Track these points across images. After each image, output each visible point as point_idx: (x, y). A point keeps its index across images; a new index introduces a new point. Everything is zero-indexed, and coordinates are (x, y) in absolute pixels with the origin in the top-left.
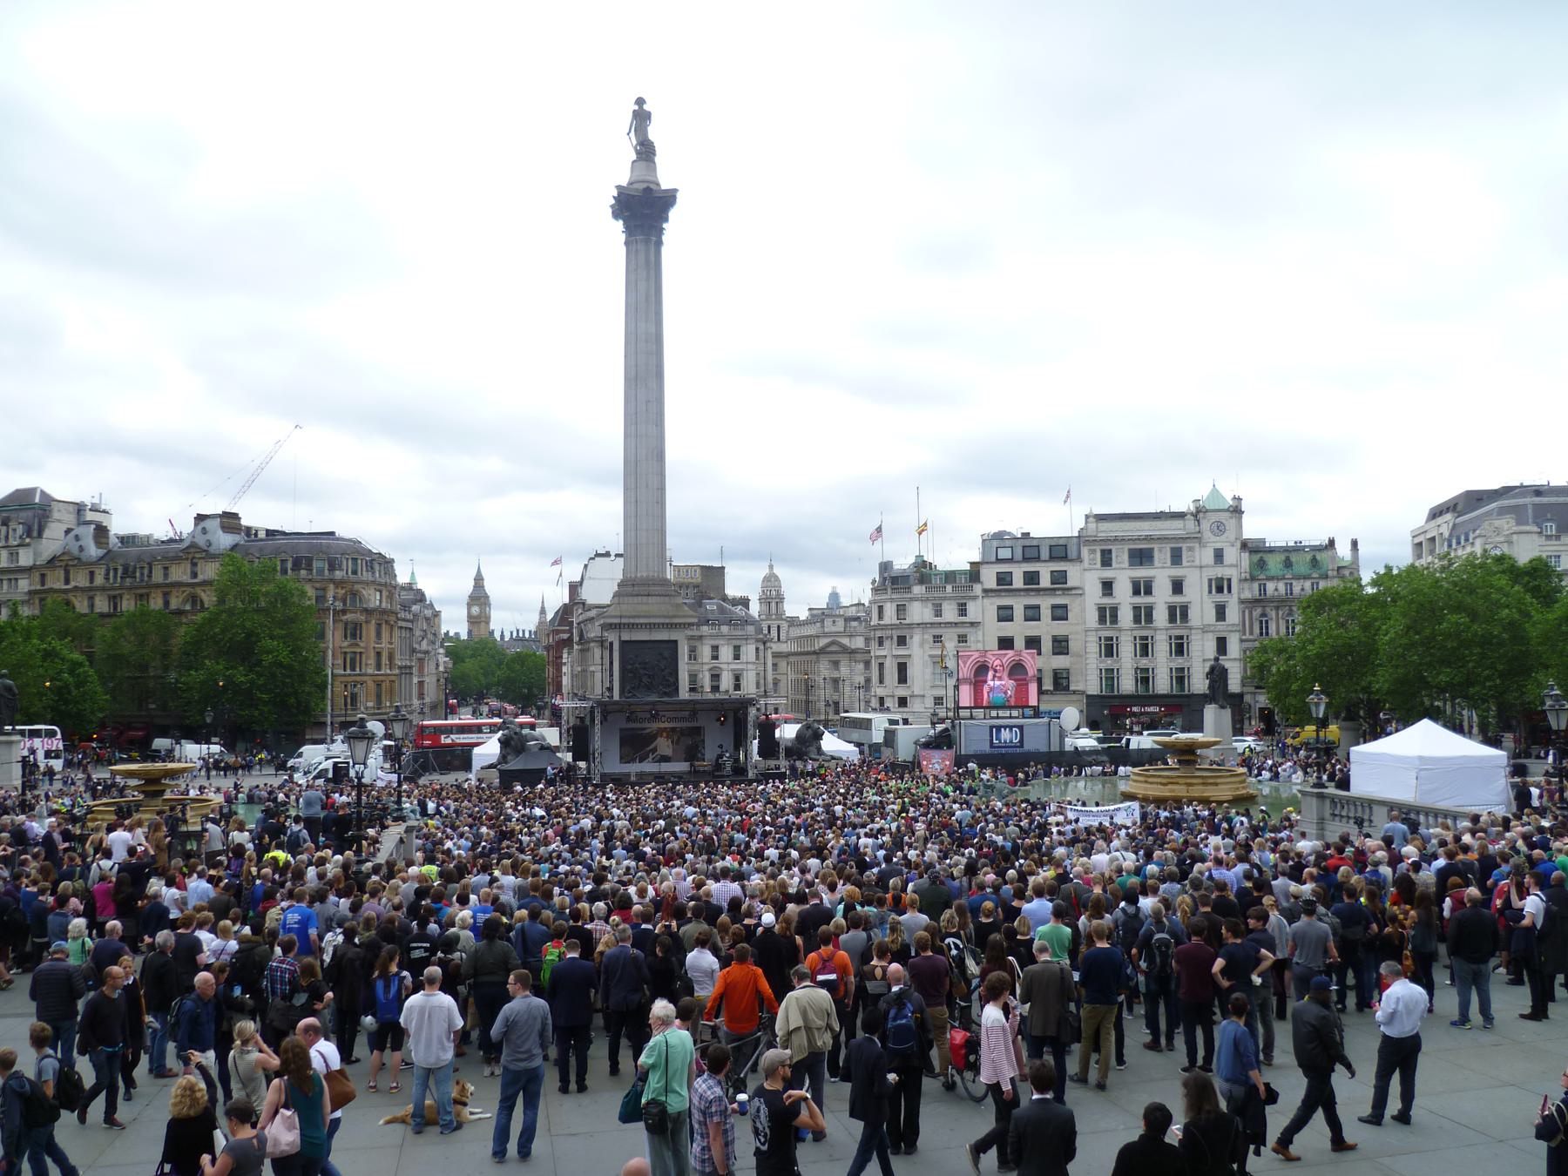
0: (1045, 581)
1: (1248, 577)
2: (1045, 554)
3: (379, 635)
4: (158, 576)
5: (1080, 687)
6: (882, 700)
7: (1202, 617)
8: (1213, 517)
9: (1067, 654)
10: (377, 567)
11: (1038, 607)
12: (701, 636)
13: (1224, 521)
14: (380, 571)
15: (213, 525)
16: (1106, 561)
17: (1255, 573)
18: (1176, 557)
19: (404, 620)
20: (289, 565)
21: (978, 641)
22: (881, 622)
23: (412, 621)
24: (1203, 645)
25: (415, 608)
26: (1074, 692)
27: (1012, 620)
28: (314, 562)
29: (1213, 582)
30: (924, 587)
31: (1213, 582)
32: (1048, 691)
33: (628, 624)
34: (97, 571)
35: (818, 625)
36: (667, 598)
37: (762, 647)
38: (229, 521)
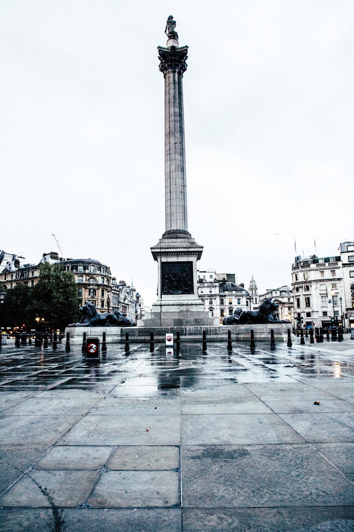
3: (103, 295)
4: (30, 276)
10: (102, 269)
12: (225, 296)
14: (103, 271)
15: (48, 257)
19: (114, 290)
20: (70, 268)
22: (297, 281)
23: (119, 291)
25: (121, 287)
28: (78, 267)
30: (315, 265)
33: (165, 252)
34: (14, 275)
35: (270, 294)
36: (186, 240)
38: (54, 255)
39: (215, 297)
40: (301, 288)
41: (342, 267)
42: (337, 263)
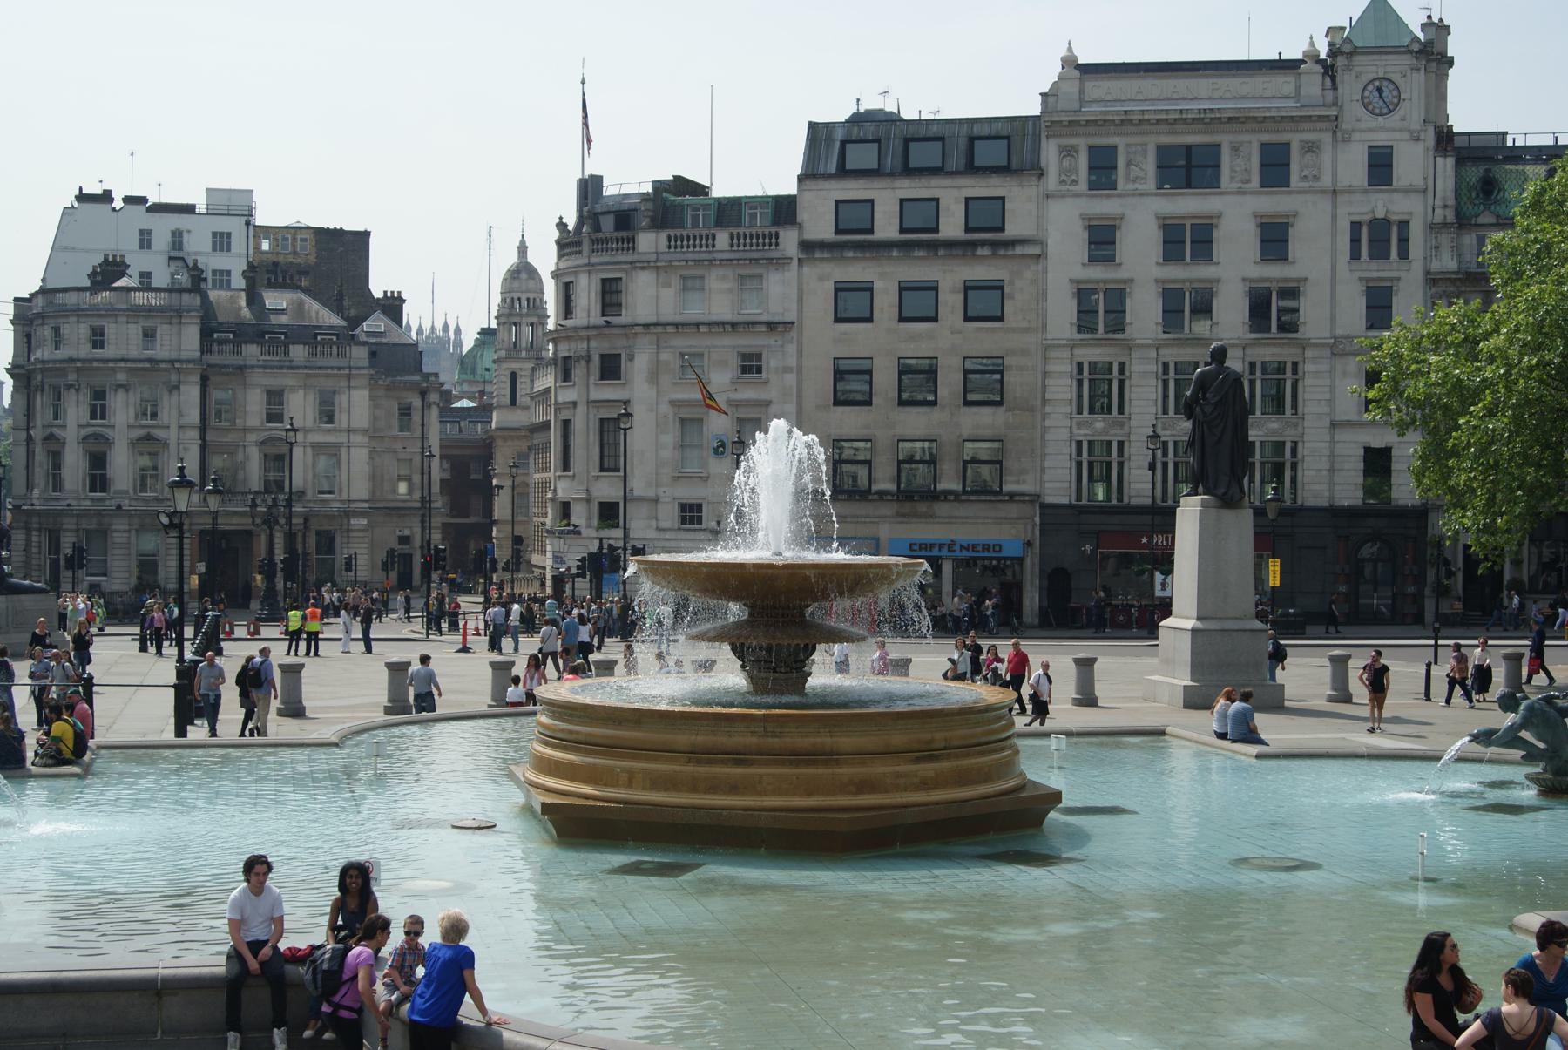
0: (952, 226)
1: (1451, 216)
2: (956, 160)
5: (1028, 487)
6: (565, 509)
7: (1333, 319)
8: (1370, 68)
9: (999, 403)
11: (933, 288)
12: (242, 368)
13: (1396, 78)
16: (1103, 170)
17: (1469, 209)
18: (1275, 169)
21: (787, 370)
22: (569, 323)
24: (1332, 389)
26: (1012, 496)
27: (870, 320)
29: (1365, 230)
30: (663, 236)
31: (1365, 230)
32: (947, 493)
37: (417, 402)
39: (174, 378)
40: (583, 363)
41: (795, 262)
42: (777, 238)
